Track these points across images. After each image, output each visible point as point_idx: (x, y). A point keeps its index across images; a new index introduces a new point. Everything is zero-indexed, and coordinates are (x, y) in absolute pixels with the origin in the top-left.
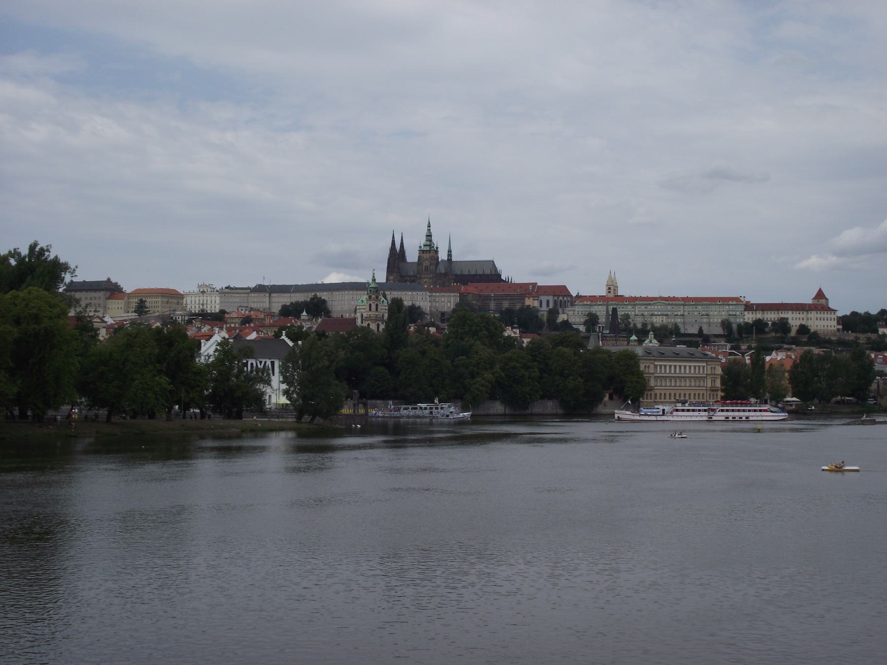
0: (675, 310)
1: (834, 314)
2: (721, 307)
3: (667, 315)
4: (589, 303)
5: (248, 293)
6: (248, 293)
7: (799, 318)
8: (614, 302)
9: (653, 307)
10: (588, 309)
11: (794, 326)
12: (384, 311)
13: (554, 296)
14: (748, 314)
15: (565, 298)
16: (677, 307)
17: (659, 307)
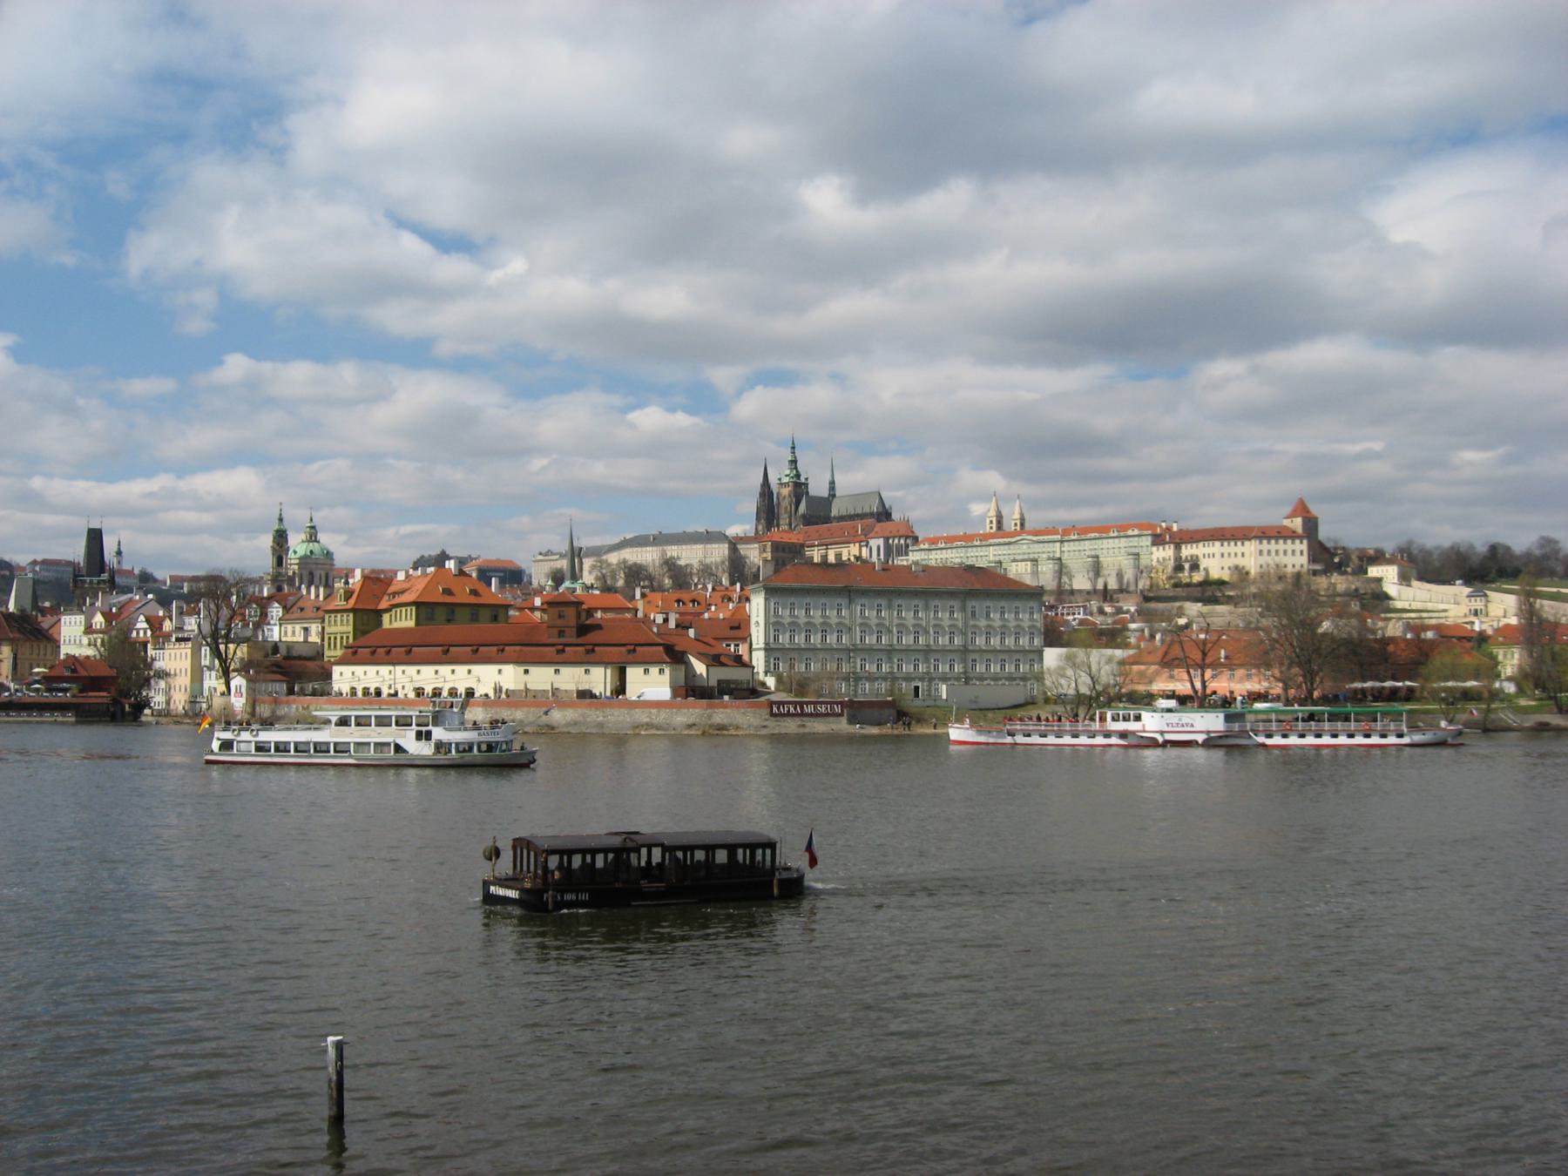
0: (1034, 551)
1: (1301, 543)
2: (1117, 540)
3: (1037, 561)
4: (926, 546)
5: (556, 560)
6: (556, 560)
7: (1236, 554)
8: (959, 543)
9: (1017, 547)
10: (926, 557)
11: (1226, 568)
12: (314, 566)
13: (887, 539)
14: (1158, 550)
15: (902, 541)
16: (1051, 544)
17: (1025, 547)
